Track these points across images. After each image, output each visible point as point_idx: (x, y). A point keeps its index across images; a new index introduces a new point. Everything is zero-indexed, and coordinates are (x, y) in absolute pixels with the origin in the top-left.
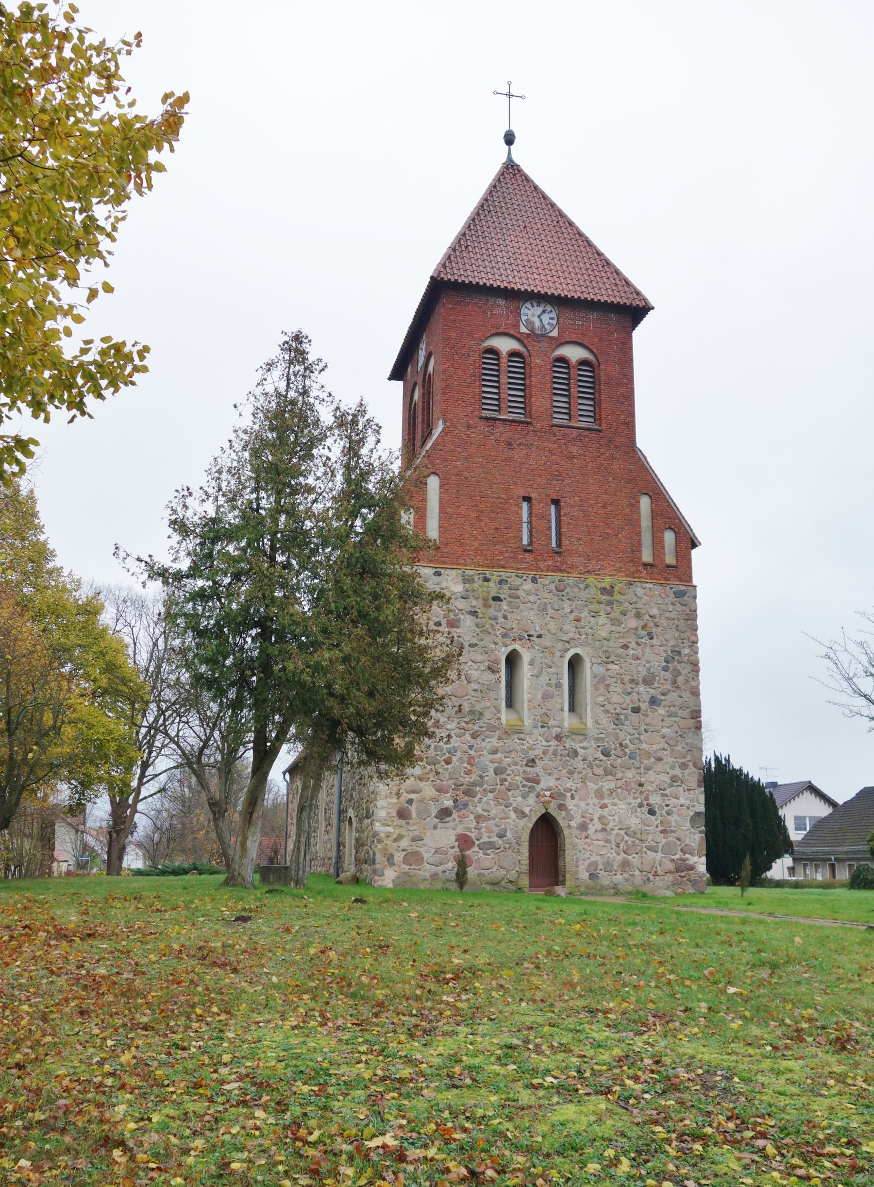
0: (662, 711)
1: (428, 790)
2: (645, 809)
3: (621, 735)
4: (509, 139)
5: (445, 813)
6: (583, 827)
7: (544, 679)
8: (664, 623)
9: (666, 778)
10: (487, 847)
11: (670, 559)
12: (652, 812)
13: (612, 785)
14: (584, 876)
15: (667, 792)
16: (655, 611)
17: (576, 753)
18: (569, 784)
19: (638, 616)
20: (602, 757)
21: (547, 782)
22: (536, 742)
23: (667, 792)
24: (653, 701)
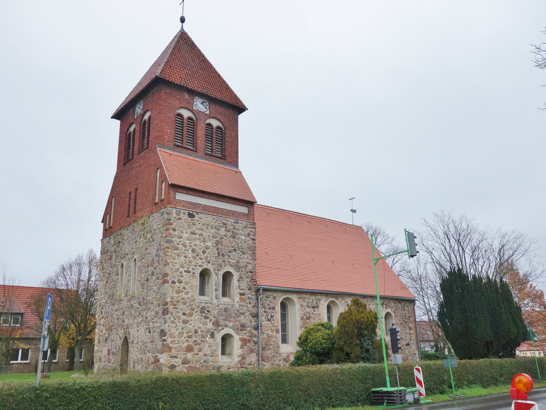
0: (154, 278)
1: (104, 331)
2: (147, 331)
3: (143, 295)
4: (183, 20)
5: (106, 340)
6: (133, 342)
7: (128, 273)
8: (157, 231)
9: (153, 313)
10: (114, 353)
11: (163, 197)
12: (149, 332)
13: (140, 320)
14: (132, 365)
15: (154, 321)
16: (155, 227)
17: (132, 305)
18: (131, 321)
19: (150, 232)
20: (139, 307)
21: (126, 322)
22: (125, 303)
23: (154, 321)
24: (153, 274)
